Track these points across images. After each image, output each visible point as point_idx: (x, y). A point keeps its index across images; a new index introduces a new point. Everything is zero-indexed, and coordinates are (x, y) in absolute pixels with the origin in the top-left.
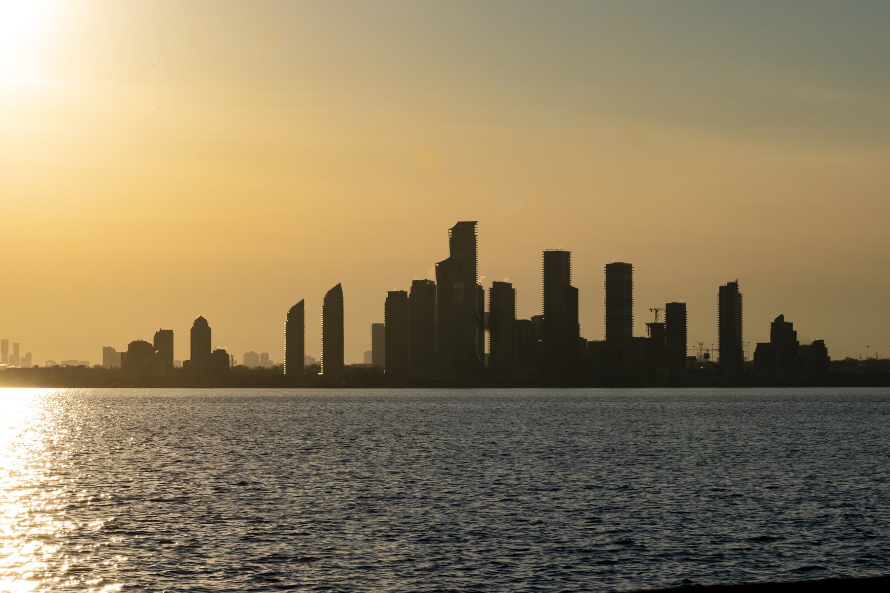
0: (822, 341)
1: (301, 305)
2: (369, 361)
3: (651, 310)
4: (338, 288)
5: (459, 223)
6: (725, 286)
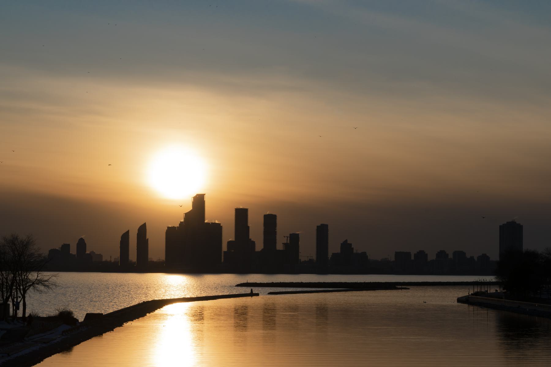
0: (366, 252)
1: (127, 233)
2: (149, 260)
3: (285, 237)
4: (144, 225)
5: (197, 195)
6: (320, 226)
